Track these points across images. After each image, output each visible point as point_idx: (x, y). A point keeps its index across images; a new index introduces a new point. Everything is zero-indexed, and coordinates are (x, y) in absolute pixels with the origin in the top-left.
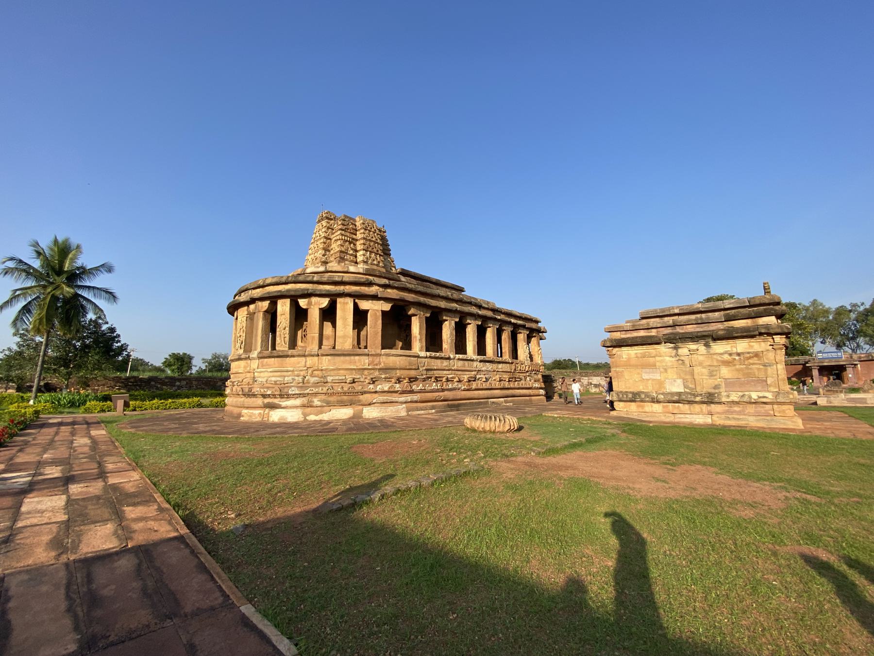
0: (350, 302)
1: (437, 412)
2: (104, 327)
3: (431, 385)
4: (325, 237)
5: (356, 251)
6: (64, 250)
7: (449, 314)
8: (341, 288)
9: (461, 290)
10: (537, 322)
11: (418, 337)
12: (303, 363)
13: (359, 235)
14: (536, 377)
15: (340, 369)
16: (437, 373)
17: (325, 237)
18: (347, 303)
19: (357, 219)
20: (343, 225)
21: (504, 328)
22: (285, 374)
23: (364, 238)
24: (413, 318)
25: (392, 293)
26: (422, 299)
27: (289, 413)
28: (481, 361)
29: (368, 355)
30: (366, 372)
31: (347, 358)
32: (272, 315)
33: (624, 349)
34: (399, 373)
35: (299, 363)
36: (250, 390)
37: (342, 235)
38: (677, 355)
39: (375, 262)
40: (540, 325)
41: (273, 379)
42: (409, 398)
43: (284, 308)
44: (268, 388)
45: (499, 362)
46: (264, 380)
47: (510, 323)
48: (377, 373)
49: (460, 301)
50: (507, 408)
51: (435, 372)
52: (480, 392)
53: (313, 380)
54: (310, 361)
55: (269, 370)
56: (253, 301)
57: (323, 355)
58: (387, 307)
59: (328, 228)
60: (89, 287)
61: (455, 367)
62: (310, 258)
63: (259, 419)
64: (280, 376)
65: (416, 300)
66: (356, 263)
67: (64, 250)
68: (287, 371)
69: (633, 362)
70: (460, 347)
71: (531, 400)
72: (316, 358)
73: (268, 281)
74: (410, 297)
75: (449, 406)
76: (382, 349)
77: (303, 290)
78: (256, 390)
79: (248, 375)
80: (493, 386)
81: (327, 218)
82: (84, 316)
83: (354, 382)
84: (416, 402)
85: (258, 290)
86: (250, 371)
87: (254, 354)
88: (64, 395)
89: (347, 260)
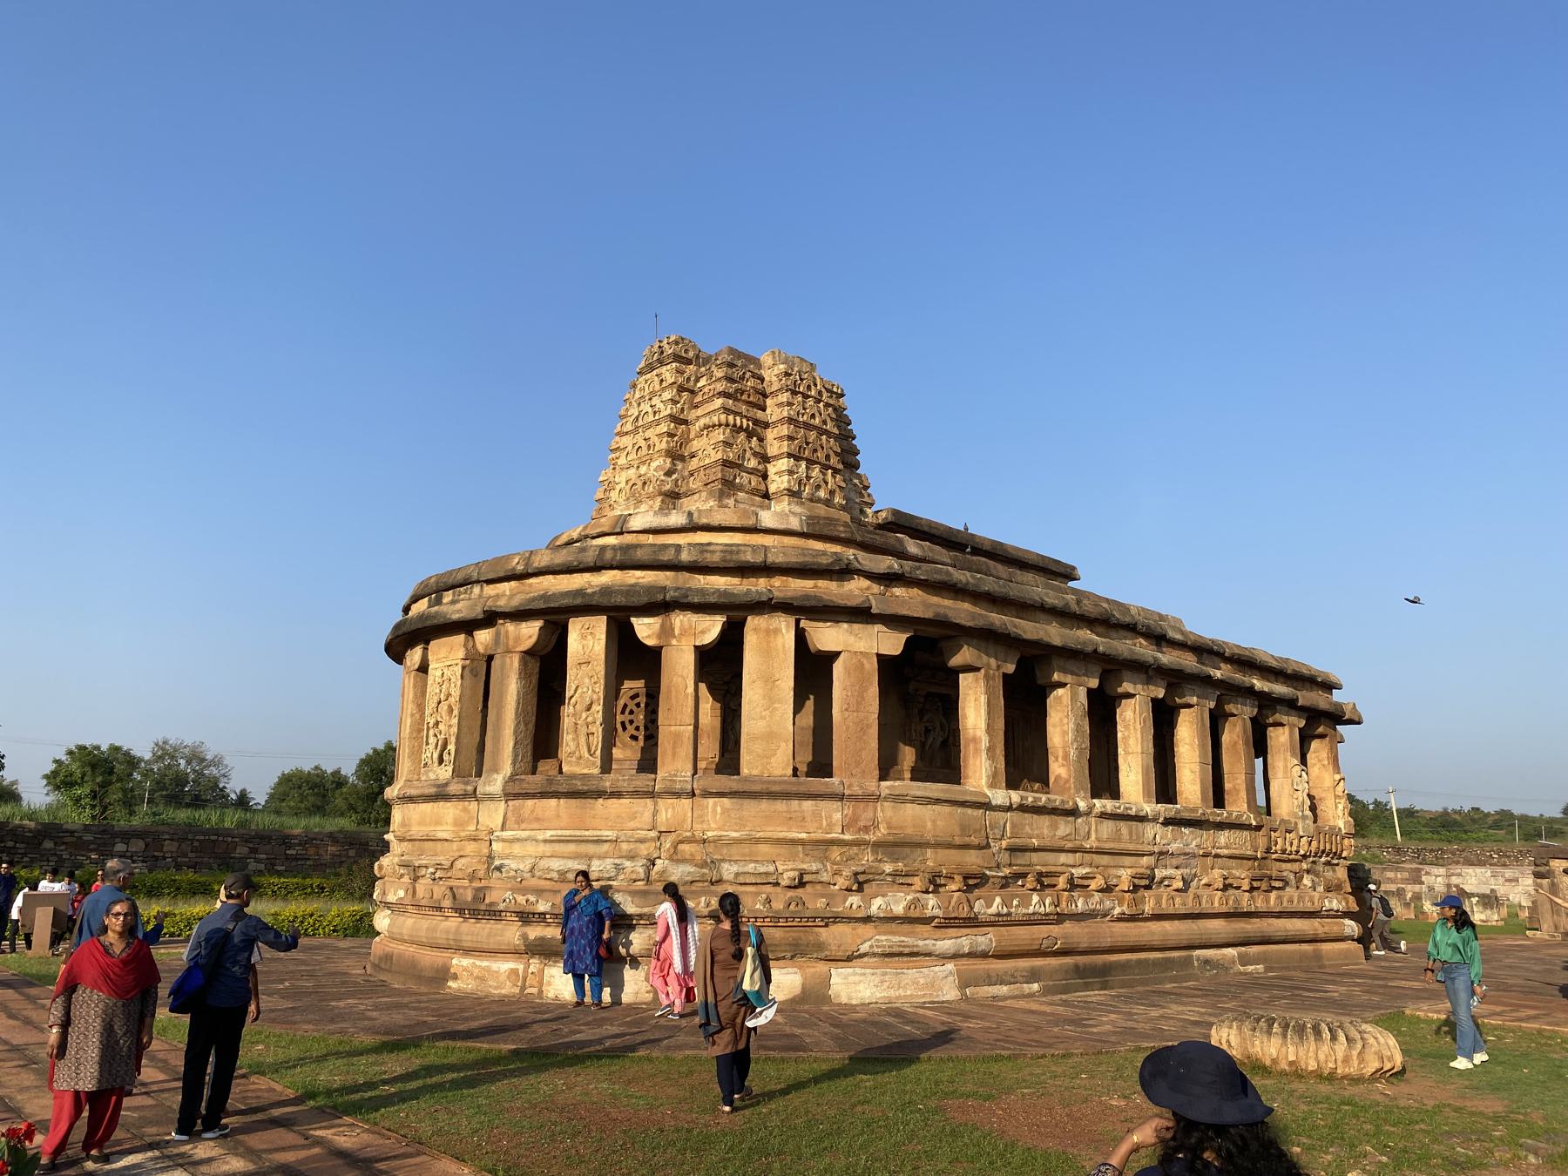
0: (783, 630)
1: (1046, 991)
3: (1026, 902)
4: (674, 418)
5: (765, 459)
7: (1070, 665)
8: (760, 586)
9: (1068, 574)
10: (1329, 686)
11: (985, 741)
12: (647, 816)
13: (774, 411)
14: (1329, 874)
15: (758, 841)
16: (1039, 862)
17: (674, 418)
18: (777, 631)
19: (766, 359)
20: (730, 379)
21: (1230, 708)
22: (591, 849)
23: (790, 420)
24: (965, 680)
25: (909, 600)
26: (997, 619)
28: (1168, 822)
29: (841, 797)
30: (835, 853)
31: (780, 806)
32: (548, 667)
34: (931, 859)
35: (633, 817)
36: (480, 894)
37: (727, 411)
39: (822, 494)
40: (1337, 696)
41: (556, 864)
42: (965, 941)
43: (587, 642)
44: (539, 892)
45: (1221, 826)
46: (525, 866)
47: (1250, 692)
48: (868, 858)
49: (1063, 615)
50: (1255, 983)
51: (1035, 857)
52: (1167, 926)
54: (670, 811)
55: (541, 836)
56: (490, 618)
57: (707, 794)
58: (892, 643)
59: (681, 389)
62: (621, 478)
63: (509, 989)
64: (576, 856)
65: (979, 623)
68: (599, 841)
70: (1102, 774)
71: (1318, 956)
72: (687, 802)
73: (542, 560)
74: (962, 611)
75: (1077, 966)
77: (650, 589)
78: (500, 895)
79: (470, 847)
80: (1205, 907)
81: (677, 358)
83: (802, 884)
84: (984, 955)
85: (506, 587)
87: (494, 783)
89: (741, 488)
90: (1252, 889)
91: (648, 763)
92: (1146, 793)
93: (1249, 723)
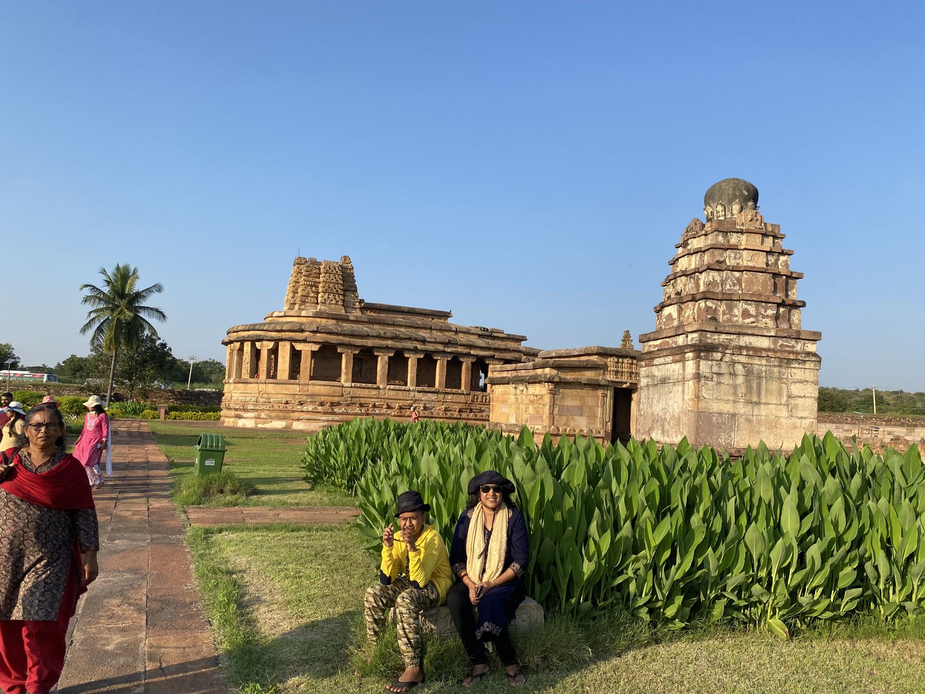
2: (158, 342)
6: (124, 276)
9: (446, 315)
13: (321, 279)
16: (363, 401)
21: (461, 360)
25: (319, 337)
26: (347, 340)
27: (247, 422)
28: (419, 392)
34: (323, 399)
38: (516, 394)
42: (330, 418)
47: (469, 355)
48: (304, 398)
53: (261, 400)
56: (231, 342)
58: (316, 348)
60: (144, 308)
61: (386, 396)
63: (231, 425)
66: (317, 303)
67: (124, 276)
69: (500, 398)
76: (312, 378)
78: (232, 406)
82: (142, 331)
86: (233, 392)
87: (231, 381)
88: (129, 404)
90: (460, 411)
91: (258, 377)
92: (412, 385)
93: (470, 365)
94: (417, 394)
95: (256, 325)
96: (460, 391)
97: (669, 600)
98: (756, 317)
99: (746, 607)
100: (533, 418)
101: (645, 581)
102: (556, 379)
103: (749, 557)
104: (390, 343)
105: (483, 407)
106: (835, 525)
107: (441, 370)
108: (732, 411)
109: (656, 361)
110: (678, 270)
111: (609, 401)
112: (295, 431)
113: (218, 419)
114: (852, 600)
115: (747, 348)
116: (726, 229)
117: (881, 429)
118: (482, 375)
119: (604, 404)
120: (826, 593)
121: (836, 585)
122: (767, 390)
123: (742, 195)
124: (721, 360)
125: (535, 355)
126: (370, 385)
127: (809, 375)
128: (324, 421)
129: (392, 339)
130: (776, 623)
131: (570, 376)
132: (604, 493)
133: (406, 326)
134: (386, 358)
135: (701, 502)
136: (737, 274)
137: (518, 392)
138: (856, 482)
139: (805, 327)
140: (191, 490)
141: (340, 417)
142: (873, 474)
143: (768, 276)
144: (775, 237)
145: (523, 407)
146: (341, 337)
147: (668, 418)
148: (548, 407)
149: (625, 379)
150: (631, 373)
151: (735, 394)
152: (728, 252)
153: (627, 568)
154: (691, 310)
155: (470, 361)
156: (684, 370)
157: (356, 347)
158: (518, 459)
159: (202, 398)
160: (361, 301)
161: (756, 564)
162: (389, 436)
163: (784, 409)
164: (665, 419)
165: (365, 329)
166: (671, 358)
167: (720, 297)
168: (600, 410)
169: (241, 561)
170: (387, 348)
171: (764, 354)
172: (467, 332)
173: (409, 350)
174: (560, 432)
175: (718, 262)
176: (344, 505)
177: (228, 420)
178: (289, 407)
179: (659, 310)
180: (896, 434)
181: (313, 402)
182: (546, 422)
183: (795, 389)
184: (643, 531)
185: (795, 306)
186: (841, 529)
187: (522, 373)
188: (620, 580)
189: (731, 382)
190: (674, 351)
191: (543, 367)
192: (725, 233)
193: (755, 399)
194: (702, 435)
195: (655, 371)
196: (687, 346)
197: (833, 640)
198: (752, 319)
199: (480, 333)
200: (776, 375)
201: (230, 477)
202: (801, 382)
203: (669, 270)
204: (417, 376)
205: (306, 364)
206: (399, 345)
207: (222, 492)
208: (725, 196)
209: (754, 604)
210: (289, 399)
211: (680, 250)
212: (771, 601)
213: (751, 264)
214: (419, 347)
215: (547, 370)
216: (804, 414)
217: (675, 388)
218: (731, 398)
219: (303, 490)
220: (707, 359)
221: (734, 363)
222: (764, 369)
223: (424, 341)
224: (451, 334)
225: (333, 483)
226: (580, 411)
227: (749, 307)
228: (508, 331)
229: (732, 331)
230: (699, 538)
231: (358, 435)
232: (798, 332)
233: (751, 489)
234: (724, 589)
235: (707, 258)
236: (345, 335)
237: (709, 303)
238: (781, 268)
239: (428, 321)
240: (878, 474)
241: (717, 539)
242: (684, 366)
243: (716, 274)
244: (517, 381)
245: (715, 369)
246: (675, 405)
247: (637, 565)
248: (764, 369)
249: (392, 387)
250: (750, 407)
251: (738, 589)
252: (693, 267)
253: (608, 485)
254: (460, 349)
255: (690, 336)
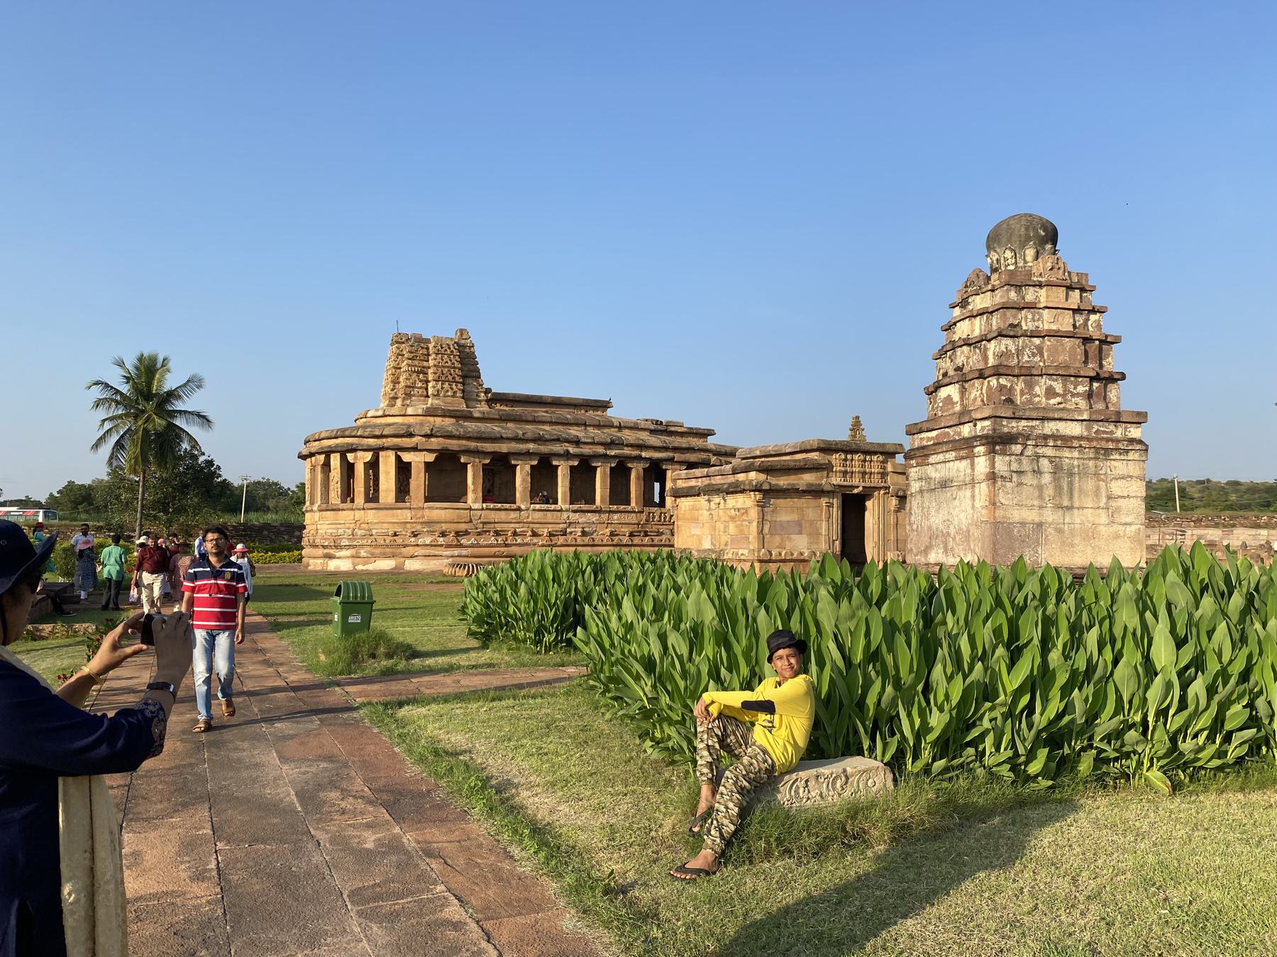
2: (201, 459)
9: (605, 405)
13: (431, 363)
16: (498, 527)
21: (630, 465)
25: (435, 443)
27: (341, 564)
28: (575, 511)
33: (683, 499)
34: (444, 527)
42: (456, 552)
43: (335, 460)
47: (639, 458)
48: (419, 527)
53: (360, 532)
54: (359, 514)
56: (312, 455)
58: (431, 458)
60: (180, 412)
63: (319, 568)
66: (427, 396)
76: (427, 499)
78: (318, 541)
86: (317, 523)
87: (315, 508)
90: (631, 535)
91: (352, 501)
92: (564, 502)
94: (571, 514)
95: (344, 430)
96: (629, 508)
97: (1031, 755)
98: (1063, 396)
99: (1116, 759)
100: (736, 541)
101: (1002, 734)
102: (766, 487)
103: (1119, 699)
104: (531, 446)
105: (662, 529)
106: (1220, 656)
107: (603, 481)
108: (1037, 520)
109: (932, 459)
110: (956, 338)
111: (836, 512)
112: (410, 572)
113: (300, 560)
114: (1241, 744)
115: (1055, 437)
116: (1018, 282)
117: (1189, 532)
118: (657, 486)
119: (829, 517)
120: (1211, 739)
121: (1222, 726)
122: (1080, 490)
123: (1037, 235)
124: (1022, 454)
125: (732, 454)
126: (507, 506)
127: (1133, 469)
128: (448, 557)
129: (534, 441)
130: (1155, 775)
131: (783, 482)
132: (941, 633)
133: (551, 423)
134: (528, 468)
135: (1058, 637)
136: (1037, 341)
137: (713, 505)
138: (1237, 601)
139: (1124, 407)
140: (335, 656)
141: (470, 550)
142: (1257, 589)
143: (1077, 341)
144: (1083, 290)
145: (720, 526)
146: (464, 442)
147: (952, 531)
148: (755, 524)
149: (856, 481)
150: (864, 473)
151: (1041, 497)
152: (1023, 312)
153: (981, 718)
154: (977, 391)
155: (646, 466)
156: (973, 469)
157: (484, 454)
158: (823, 593)
159: (265, 533)
160: (488, 391)
161: (1126, 707)
162: (583, 573)
163: (1103, 513)
164: (949, 534)
165: (496, 428)
166: (954, 454)
167: (1016, 372)
168: (824, 524)
169: (458, 739)
170: (528, 454)
171: (1076, 444)
172: (635, 427)
173: (558, 455)
174: (774, 558)
175: (1012, 326)
176: (536, 664)
177: (314, 562)
178: (399, 540)
179: (933, 391)
180: (1209, 538)
181: (431, 532)
182: (754, 545)
183: (1117, 488)
184: (995, 676)
185: (1112, 379)
186: (1226, 659)
187: (718, 480)
188: (975, 733)
189: (1035, 482)
190: (957, 445)
191: (746, 471)
192: (1018, 287)
193: (1066, 503)
194: (1001, 552)
195: (930, 471)
196: (975, 438)
197: (1222, 792)
198: (1059, 399)
199: (652, 427)
200: (1092, 470)
201: (381, 637)
202: (1123, 478)
203: (942, 339)
204: (571, 489)
205: (418, 481)
206: (544, 449)
207: (373, 656)
208: (1015, 238)
209: (1127, 756)
210: (398, 529)
211: (957, 312)
212: (1147, 751)
213: (1054, 327)
214: (572, 450)
215: (753, 475)
216: (1128, 520)
217: (960, 493)
218: (1036, 503)
219: (474, 649)
220: (1004, 453)
221: (1038, 457)
222: (1076, 463)
223: (577, 442)
224: (613, 431)
225: (515, 638)
226: (799, 527)
227: (1054, 384)
228: (690, 423)
229: (1034, 415)
230: (1062, 679)
231: (542, 573)
232: (1118, 413)
233: (1110, 617)
234: (1091, 738)
235: (996, 321)
236: (469, 439)
237: (1003, 381)
238: (1092, 330)
239: (581, 414)
240: (1262, 591)
241: (1081, 678)
242: (972, 465)
243: (1009, 341)
244: (711, 491)
245: (1015, 466)
246: (962, 516)
247: (993, 714)
248: (1076, 463)
249: (538, 506)
250: (1060, 512)
251: (1108, 738)
252: (977, 333)
253: (944, 623)
254: (627, 451)
255: (979, 425)
